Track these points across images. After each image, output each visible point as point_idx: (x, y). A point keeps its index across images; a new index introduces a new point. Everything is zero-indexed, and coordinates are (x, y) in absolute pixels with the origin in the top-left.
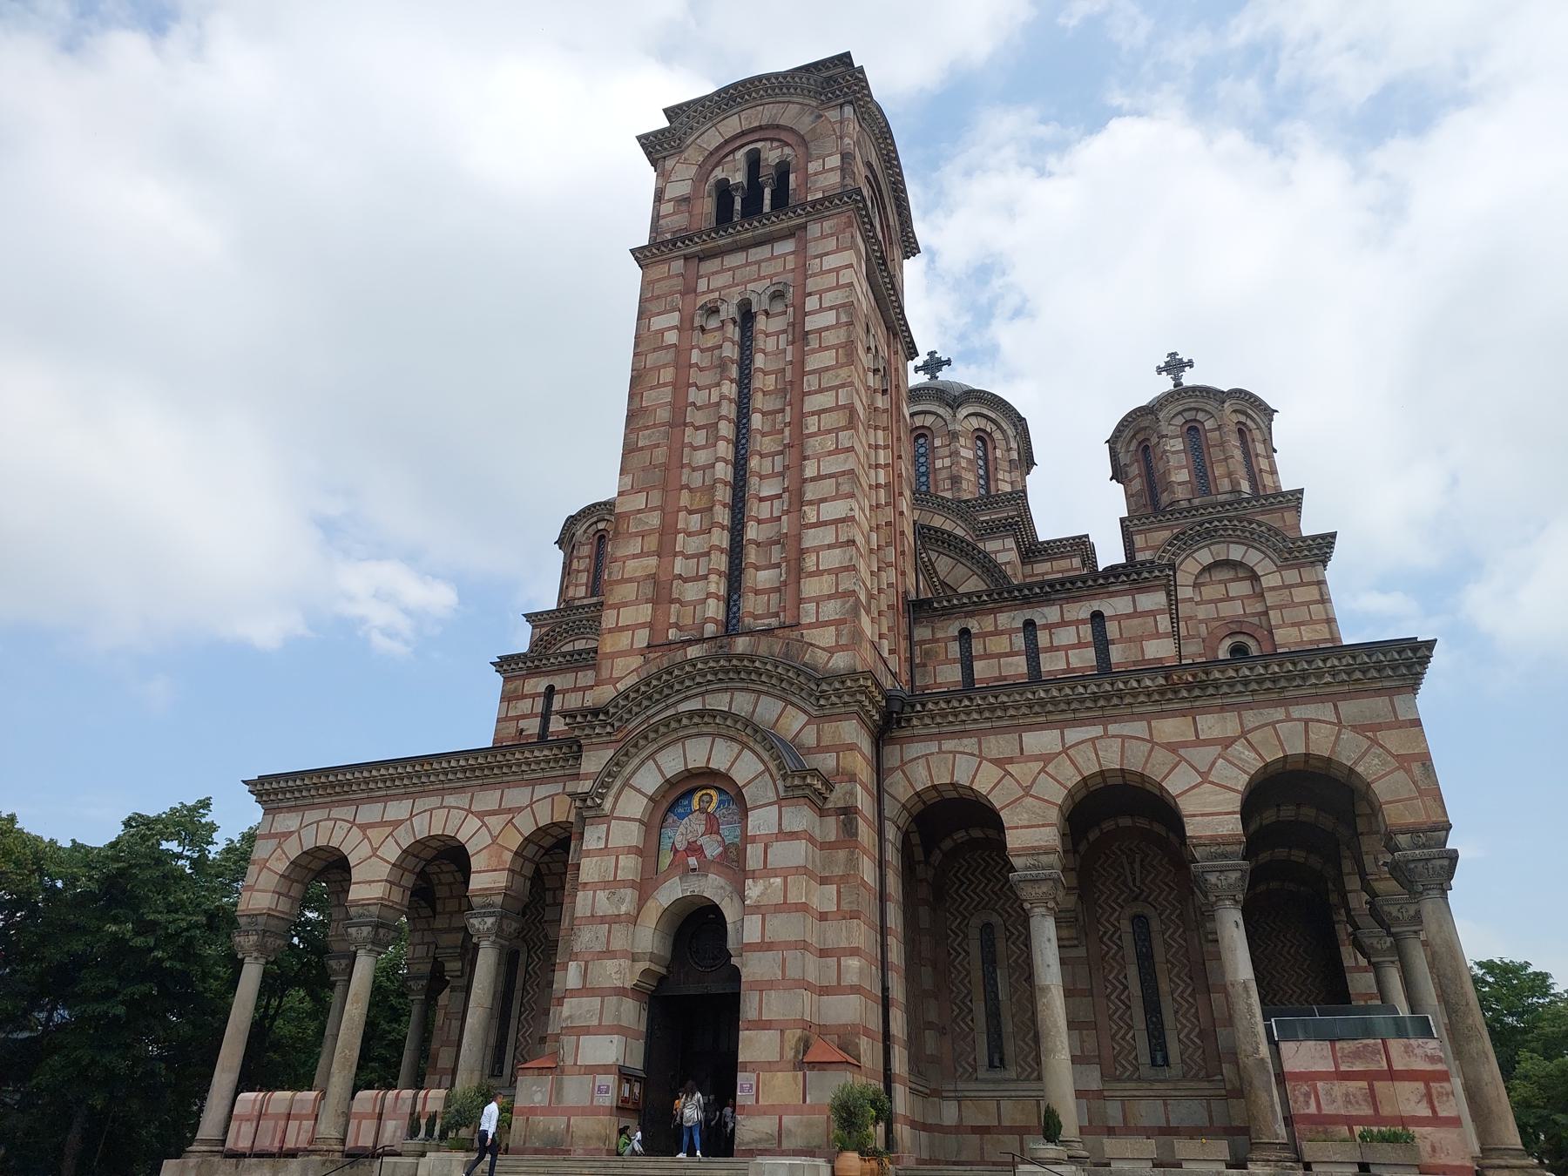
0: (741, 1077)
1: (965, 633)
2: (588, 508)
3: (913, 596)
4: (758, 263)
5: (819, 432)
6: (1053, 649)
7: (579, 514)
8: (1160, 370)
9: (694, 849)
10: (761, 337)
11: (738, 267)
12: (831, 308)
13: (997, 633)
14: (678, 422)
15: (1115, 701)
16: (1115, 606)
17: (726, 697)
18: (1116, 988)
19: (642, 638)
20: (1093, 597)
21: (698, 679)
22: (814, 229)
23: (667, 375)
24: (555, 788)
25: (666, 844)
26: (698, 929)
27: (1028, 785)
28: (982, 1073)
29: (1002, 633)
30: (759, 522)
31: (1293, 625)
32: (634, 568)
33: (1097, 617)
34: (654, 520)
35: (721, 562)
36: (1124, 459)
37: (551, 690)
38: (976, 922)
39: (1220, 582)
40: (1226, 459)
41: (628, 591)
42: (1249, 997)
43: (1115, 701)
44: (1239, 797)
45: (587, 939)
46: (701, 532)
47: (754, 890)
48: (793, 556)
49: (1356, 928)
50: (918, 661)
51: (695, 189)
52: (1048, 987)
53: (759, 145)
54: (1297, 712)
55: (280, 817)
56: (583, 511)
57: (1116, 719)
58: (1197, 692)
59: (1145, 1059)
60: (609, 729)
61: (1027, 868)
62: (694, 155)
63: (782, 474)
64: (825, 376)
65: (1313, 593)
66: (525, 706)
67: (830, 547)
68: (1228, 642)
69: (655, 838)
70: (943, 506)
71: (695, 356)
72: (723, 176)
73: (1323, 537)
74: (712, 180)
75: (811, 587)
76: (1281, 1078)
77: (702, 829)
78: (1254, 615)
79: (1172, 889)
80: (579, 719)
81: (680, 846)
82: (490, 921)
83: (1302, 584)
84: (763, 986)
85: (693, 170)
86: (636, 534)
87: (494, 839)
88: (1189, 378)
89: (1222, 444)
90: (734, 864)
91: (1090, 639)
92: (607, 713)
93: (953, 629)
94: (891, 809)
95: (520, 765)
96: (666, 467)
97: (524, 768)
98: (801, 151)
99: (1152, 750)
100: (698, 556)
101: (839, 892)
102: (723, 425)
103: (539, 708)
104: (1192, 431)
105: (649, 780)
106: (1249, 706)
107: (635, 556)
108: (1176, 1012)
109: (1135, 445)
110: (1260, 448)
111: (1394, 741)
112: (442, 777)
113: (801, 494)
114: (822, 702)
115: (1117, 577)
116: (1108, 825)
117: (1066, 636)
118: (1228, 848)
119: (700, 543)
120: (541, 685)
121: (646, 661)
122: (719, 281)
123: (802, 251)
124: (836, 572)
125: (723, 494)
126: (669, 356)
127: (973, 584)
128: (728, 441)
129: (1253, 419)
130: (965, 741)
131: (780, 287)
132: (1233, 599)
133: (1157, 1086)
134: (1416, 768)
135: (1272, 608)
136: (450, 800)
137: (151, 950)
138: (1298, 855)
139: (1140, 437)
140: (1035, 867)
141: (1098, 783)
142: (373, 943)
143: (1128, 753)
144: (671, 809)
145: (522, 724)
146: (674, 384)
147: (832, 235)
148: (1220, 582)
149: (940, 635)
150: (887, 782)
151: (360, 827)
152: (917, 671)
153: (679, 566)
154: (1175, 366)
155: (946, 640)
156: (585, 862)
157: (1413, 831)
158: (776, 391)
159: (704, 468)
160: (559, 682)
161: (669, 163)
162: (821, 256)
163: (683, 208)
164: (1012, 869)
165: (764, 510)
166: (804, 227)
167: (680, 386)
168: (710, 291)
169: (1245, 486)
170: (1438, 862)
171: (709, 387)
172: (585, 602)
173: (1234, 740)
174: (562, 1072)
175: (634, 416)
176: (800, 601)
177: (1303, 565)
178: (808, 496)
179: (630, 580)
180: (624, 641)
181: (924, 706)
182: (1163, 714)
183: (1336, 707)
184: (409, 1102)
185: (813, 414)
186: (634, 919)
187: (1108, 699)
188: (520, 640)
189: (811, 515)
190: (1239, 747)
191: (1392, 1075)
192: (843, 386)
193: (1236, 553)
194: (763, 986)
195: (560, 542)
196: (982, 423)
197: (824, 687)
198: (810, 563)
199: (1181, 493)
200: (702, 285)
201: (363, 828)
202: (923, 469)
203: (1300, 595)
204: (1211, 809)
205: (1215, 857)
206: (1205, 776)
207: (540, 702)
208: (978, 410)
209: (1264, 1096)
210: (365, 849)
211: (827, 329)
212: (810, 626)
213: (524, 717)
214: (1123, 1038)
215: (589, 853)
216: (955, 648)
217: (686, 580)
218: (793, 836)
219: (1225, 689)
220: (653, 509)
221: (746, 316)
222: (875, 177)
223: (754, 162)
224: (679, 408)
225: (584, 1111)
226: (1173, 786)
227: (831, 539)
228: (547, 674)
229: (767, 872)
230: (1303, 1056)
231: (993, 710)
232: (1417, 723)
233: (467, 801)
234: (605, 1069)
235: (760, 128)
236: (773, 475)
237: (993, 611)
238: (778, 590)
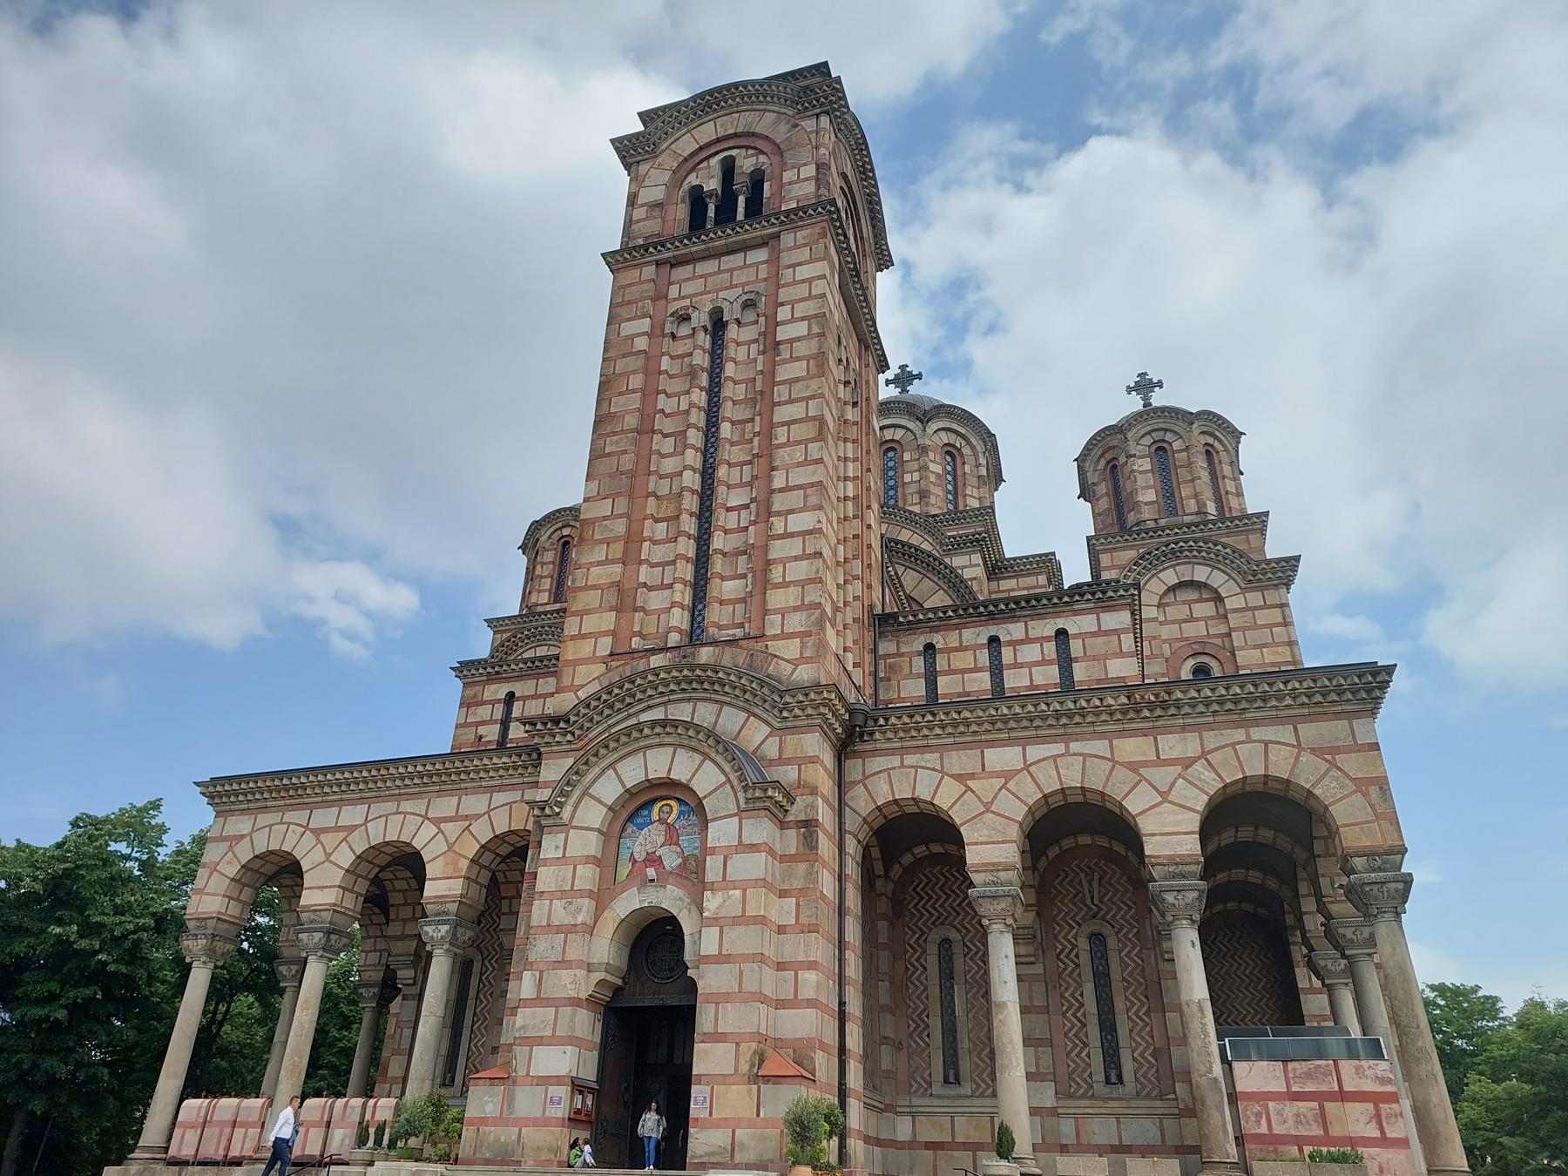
0: (695, 1090)
1: (930, 647)
2: (554, 513)
3: (878, 610)
4: (731, 271)
5: (789, 443)
6: (1016, 665)
7: (543, 519)
8: (1129, 390)
9: (653, 860)
10: (732, 346)
11: (710, 275)
12: (803, 319)
13: (961, 649)
14: (646, 429)
15: (1077, 719)
16: (1078, 624)
17: (689, 707)
18: (1072, 1005)
20: (1058, 614)
21: (661, 689)
22: (787, 239)
23: (636, 381)
24: (515, 795)
25: (625, 855)
26: (656, 940)
27: (989, 802)
28: (937, 1089)
29: (966, 649)
30: (726, 532)
31: (1255, 647)
32: (598, 575)
33: (1062, 634)
34: (620, 527)
35: (687, 571)
36: (1092, 478)
37: (511, 695)
38: (935, 937)
39: (1184, 602)
40: (1193, 480)
41: (592, 598)
42: (1203, 1016)
43: (1077, 719)
44: (1198, 817)
45: (542, 948)
46: (668, 540)
47: (712, 902)
48: (759, 566)
49: (1312, 949)
50: (882, 675)
51: (668, 194)
52: (1004, 1004)
53: (734, 152)
54: (1256, 733)
55: (232, 820)
56: (548, 516)
57: (1079, 737)
58: (1159, 712)
59: (1099, 1076)
60: (569, 737)
61: (986, 884)
62: (668, 161)
63: (750, 484)
64: (797, 387)
65: (1275, 615)
66: (484, 712)
67: (796, 558)
68: (1191, 662)
69: (615, 847)
70: (911, 520)
71: (665, 363)
73: (1287, 560)
74: (686, 186)
75: (776, 599)
76: (1233, 1097)
77: (661, 839)
78: (1216, 636)
79: (1130, 908)
80: (539, 726)
81: (639, 857)
82: (444, 929)
83: (1266, 606)
84: (719, 999)
85: (667, 176)
86: (601, 542)
87: (450, 846)
88: (1158, 399)
89: (1189, 465)
90: (693, 875)
91: (1054, 656)
92: (567, 721)
93: (918, 644)
94: (851, 823)
95: (478, 772)
96: (633, 474)
97: (482, 774)
98: (776, 159)
99: (1113, 768)
100: (663, 564)
101: (798, 905)
102: (691, 433)
103: (498, 715)
104: (1161, 451)
105: (609, 790)
106: (1210, 727)
107: (600, 563)
108: (1131, 1031)
109: (1103, 464)
110: (1227, 470)
111: (1352, 764)
112: (398, 782)
113: (769, 504)
114: (785, 714)
115: (1082, 595)
116: (1067, 843)
117: (1030, 653)
118: (1187, 868)
119: (668, 552)
120: (501, 691)
121: (609, 670)
122: (691, 288)
123: (774, 261)
124: (802, 584)
125: (691, 503)
126: (638, 362)
127: (939, 599)
128: (696, 449)
129: (1221, 442)
130: (927, 756)
131: (752, 296)
132: (1197, 619)
133: (1111, 1104)
134: (1374, 791)
135: (1235, 630)
136: (407, 806)
137: (96, 953)
138: (1255, 877)
139: (1109, 456)
140: (995, 884)
141: (1058, 801)
142: (324, 950)
143: (1089, 771)
144: (630, 819)
145: (482, 730)
146: (643, 391)
147: (805, 245)
148: (1184, 602)
149: (904, 649)
150: (848, 796)
151: (313, 831)
152: (881, 685)
153: (644, 574)
154: (1144, 386)
155: (911, 655)
156: (542, 871)
157: (1370, 854)
158: (745, 401)
159: (671, 476)
160: (519, 688)
161: (643, 168)
162: (794, 266)
163: (656, 213)
164: (972, 885)
165: (731, 521)
166: (777, 236)
167: (649, 393)
168: (681, 298)
169: (1211, 508)
170: (1393, 886)
171: (678, 395)
172: (548, 608)
173: (1194, 760)
174: (514, 1083)
175: (603, 421)
176: (765, 612)
177: (1267, 588)
178: (776, 507)
179: (594, 587)
180: (586, 648)
181: (887, 720)
182: (1123, 734)
183: (1295, 729)
184: (358, 1111)
185: (783, 424)
186: (590, 930)
187: (1070, 717)
188: (481, 645)
189: (779, 527)
190: (1199, 766)
191: (1343, 1096)
192: (813, 397)
193: (1201, 573)
194: (719, 999)
195: (524, 547)
196: (952, 438)
197: (788, 699)
198: (776, 574)
199: (1148, 513)
200: (674, 291)
201: (317, 832)
202: (891, 483)
203: (1264, 617)
204: (1171, 831)
205: (1174, 876)
206: (1164, 795)
207: (500, 708)
208: (948, 425)
209: (1216, 1118)
210: (318, 854)
211: (798, 339)
212: (775, 637)
213: (483, 723)
214: (1078, 1055)
215: (546, 862)
216: (919, 664)
217: (650, 589)
218: (753, 848)
219: (1187, 709)
220: (619, 516)
221: (718, 325)
222: (850, 188)
223: (728, 169)
224: (647, 416)
225: (535, 1123)
226: (1133, 805)
227: (798, 551)
228: (508, 680)
229: (726, 884)
230: (1256, 1075)
231: (955, 726)
232: (1375, 747)
233: (424, 807)
234: (558, 1080)
235: (736, 135)
236: (741, 485)
237: (957, 627)
238: (743, 600)
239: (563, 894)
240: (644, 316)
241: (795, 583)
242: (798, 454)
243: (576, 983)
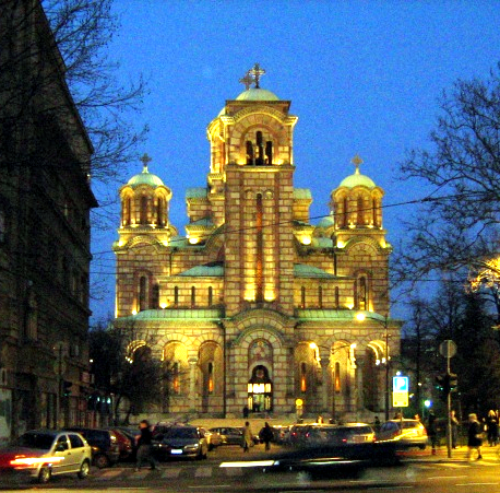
16: (342, 286)
37: (176, 289)
45: (238, 373)
47: (275, 366)
51: (241, 143)
66: (168, 292)
85: (240, 135)
122: (251, 182)
180: (232, 300)
223: (259, 134)
242: (287, 251)
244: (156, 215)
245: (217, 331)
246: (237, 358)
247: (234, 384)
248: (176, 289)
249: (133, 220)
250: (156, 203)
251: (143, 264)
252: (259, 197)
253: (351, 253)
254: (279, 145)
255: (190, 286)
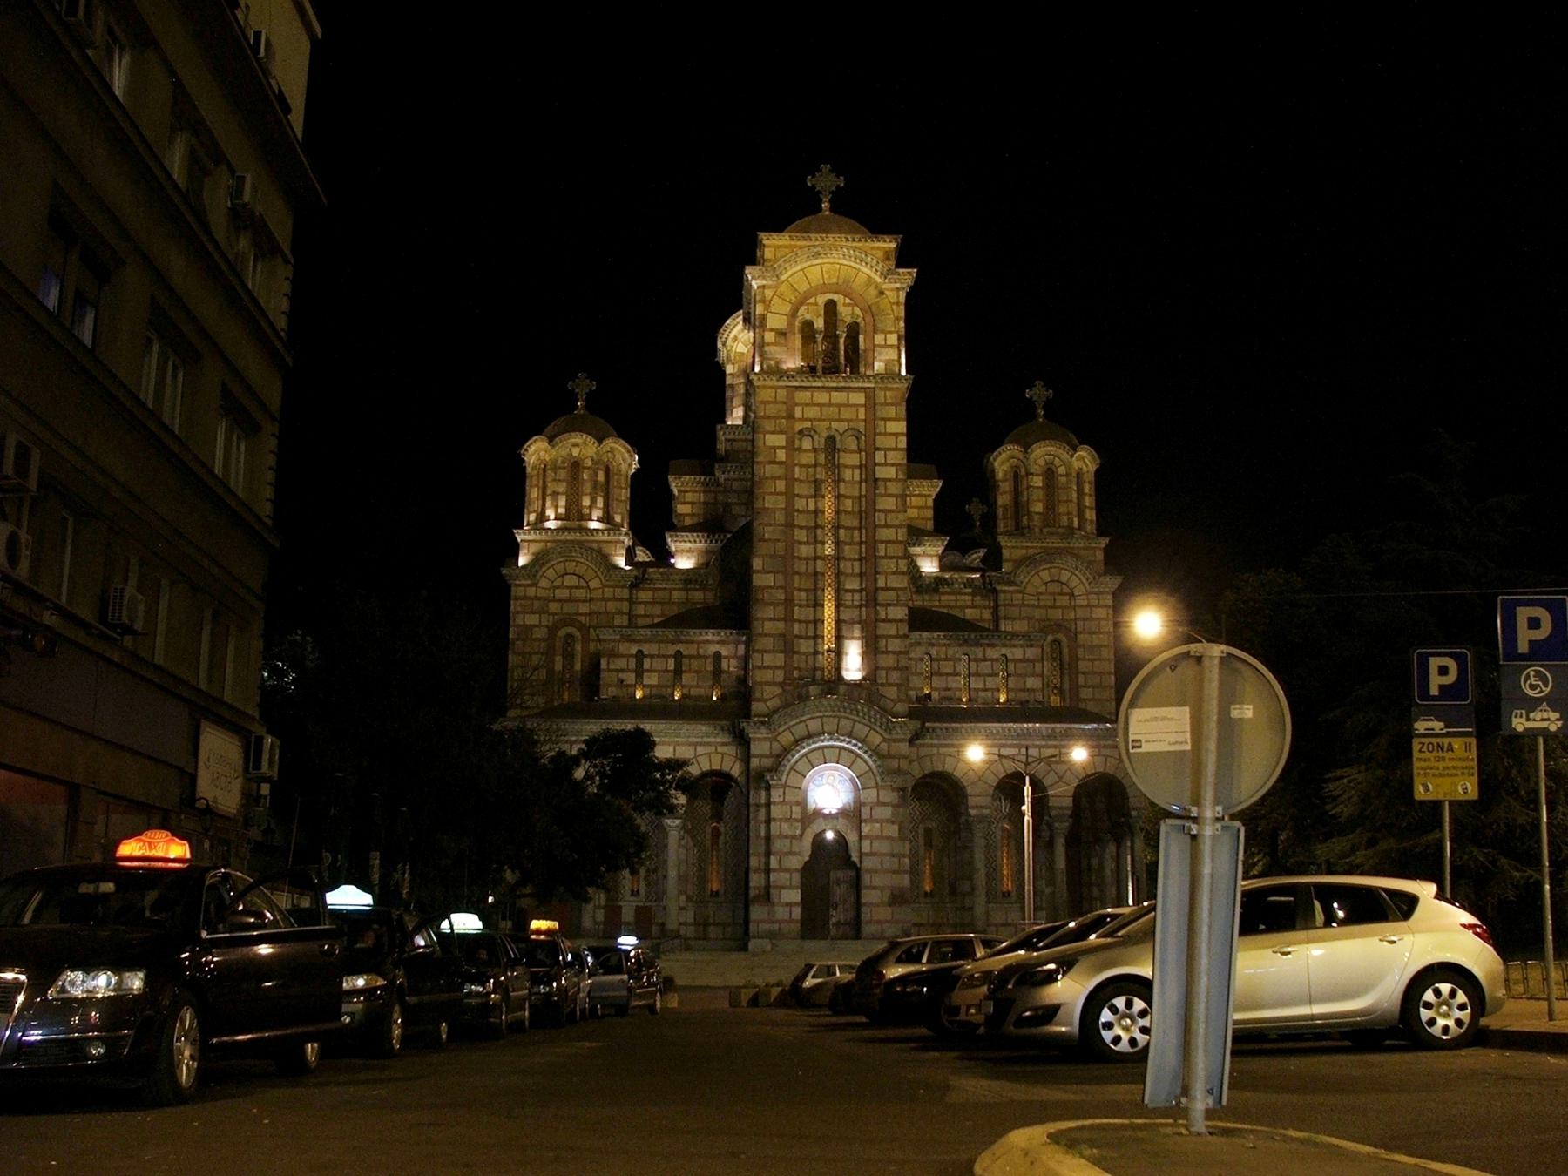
4: (839, 406)
14: (790, 525)
19: (780, 676)
20: (1005, 646)
32: (769, 627)
37: (640, 651)
41: (768, 643)
45: (778, 845)
47: (866, 829)
51: (790, 324)
64: (890, 516)
66: (621, 663)
72: (808, 317)
85: (787, 309)
98: (869, 319)
100: (807, 622)
103: (633, 663)
122: (812, 412)
145: (623, 676)
153: (797, 629)
159: (806, 559)
160: (647, 648)
167: (790, 495)
168: (803, 419)
171: (807, 497)
180: (768, 676)
186: (801, 835)
189: (882, 615)
193: (1065, 576)
194: (870, 871)
200: (798, 413)
213: (622, 671)
223: (831, 307)
224: (790, 511)
227: (893, 632)
228: (634, 641)
229: (872, 820)
236: (852, 575)
239: (787, 820)
240: (781, 432)
241: (894, 653)
243: (796, 863)
244: (600, 502)
245: (731, 750)
246: (776, 811)
247: (768, 871)
248: (640, 656)
249: (550, 513)
250: (601, 477)
251: (569, 608)
252: (831, 440)
253: (1030, 589)
254: (875, 331)
255: (671, 650)
